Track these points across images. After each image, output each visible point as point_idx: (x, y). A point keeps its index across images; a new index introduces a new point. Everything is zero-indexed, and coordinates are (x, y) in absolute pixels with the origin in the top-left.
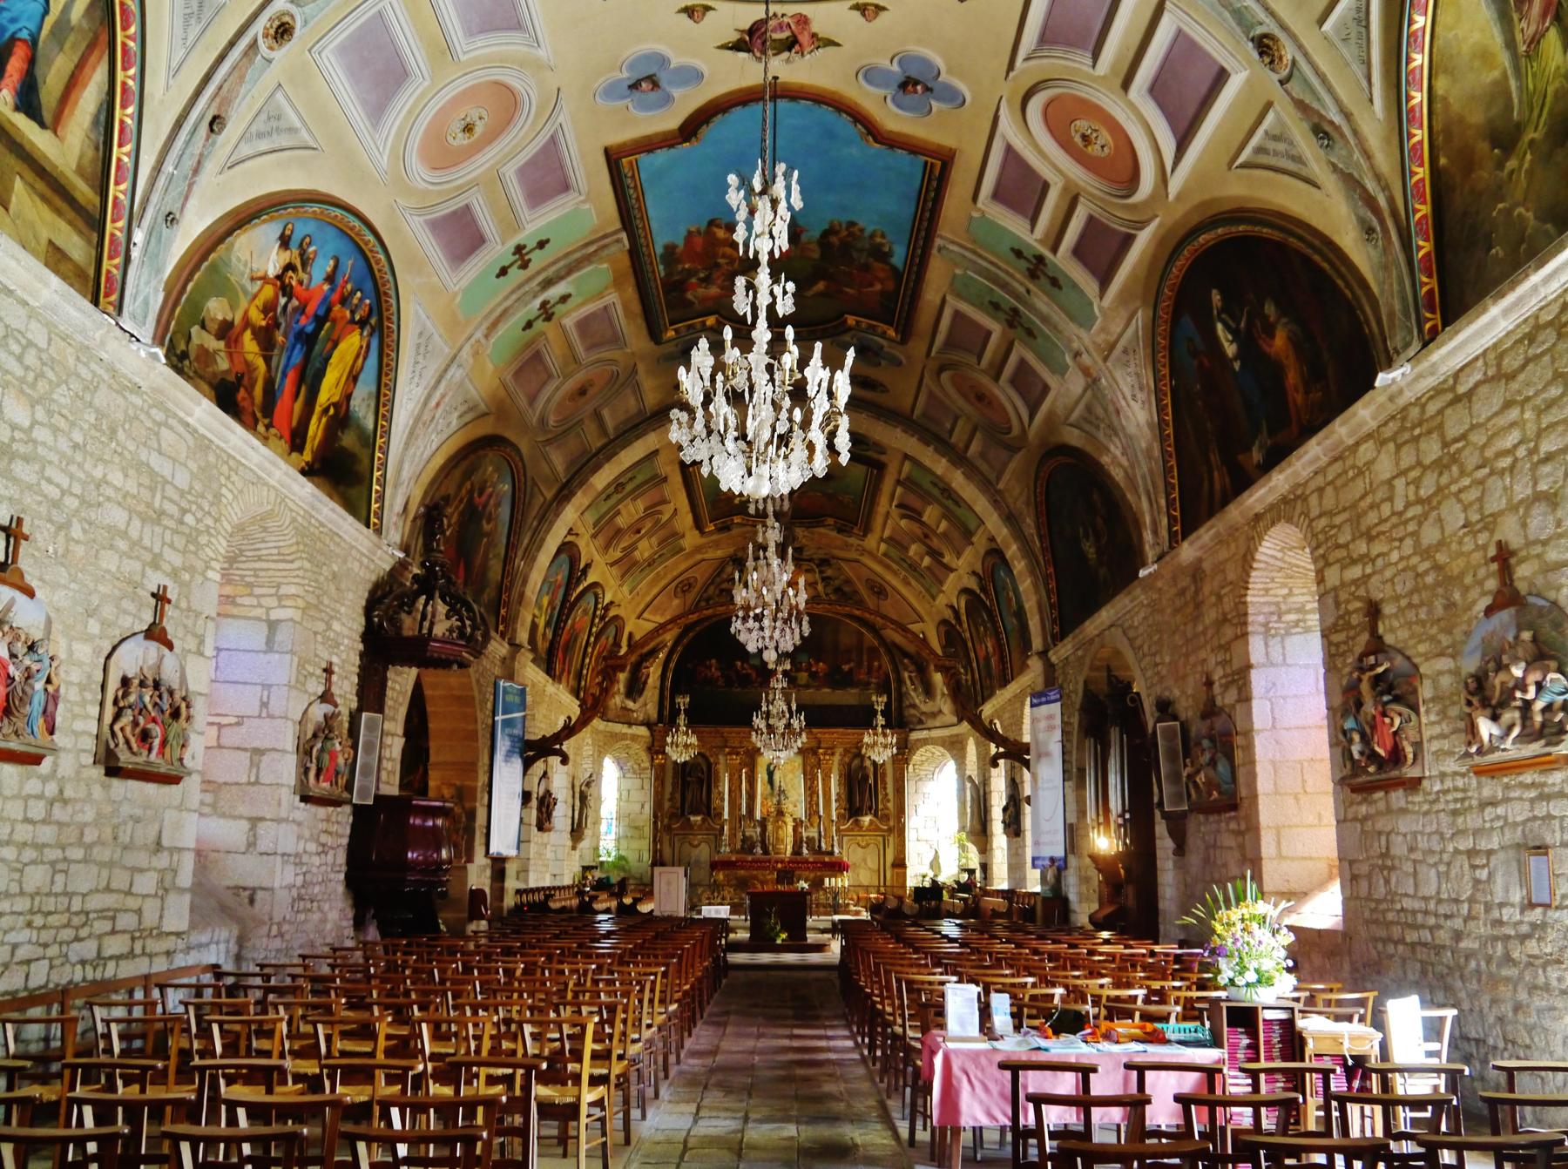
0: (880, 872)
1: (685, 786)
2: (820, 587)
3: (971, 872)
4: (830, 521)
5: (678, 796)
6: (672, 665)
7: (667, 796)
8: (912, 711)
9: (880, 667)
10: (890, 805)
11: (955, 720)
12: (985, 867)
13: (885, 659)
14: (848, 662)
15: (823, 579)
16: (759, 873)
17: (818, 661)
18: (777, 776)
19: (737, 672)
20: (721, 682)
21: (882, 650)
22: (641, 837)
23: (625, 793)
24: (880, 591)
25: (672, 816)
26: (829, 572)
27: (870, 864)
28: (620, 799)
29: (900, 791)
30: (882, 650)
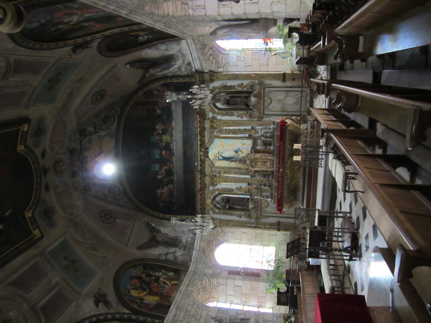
0: (288, 91)
1: (231, 208)
2: (102, 133)
3: (292, 30)
4: (21, 148)
5: (238, 213)
6: (161, 215)
7: (238, 219)
8: (183, 69)
9: (156, 90)
10: (245, 82)
11: (183, 42)
12: (288, 20)
13: (151, 86)
14: (155, 110)
15: (96, 132)
16: (286, 182)
17: (154, 129)
18: (227, 154)
19: (164, 177)
20: (171, 186)
21: (146, 89)
22: (261, 234)
23: (236, 241)
24: (100, 95)
25: (249, 216)
26: (90, 129)
27: (281, 97)
28: (240, 243)
29: (236, 77)
30: (146, 89)
